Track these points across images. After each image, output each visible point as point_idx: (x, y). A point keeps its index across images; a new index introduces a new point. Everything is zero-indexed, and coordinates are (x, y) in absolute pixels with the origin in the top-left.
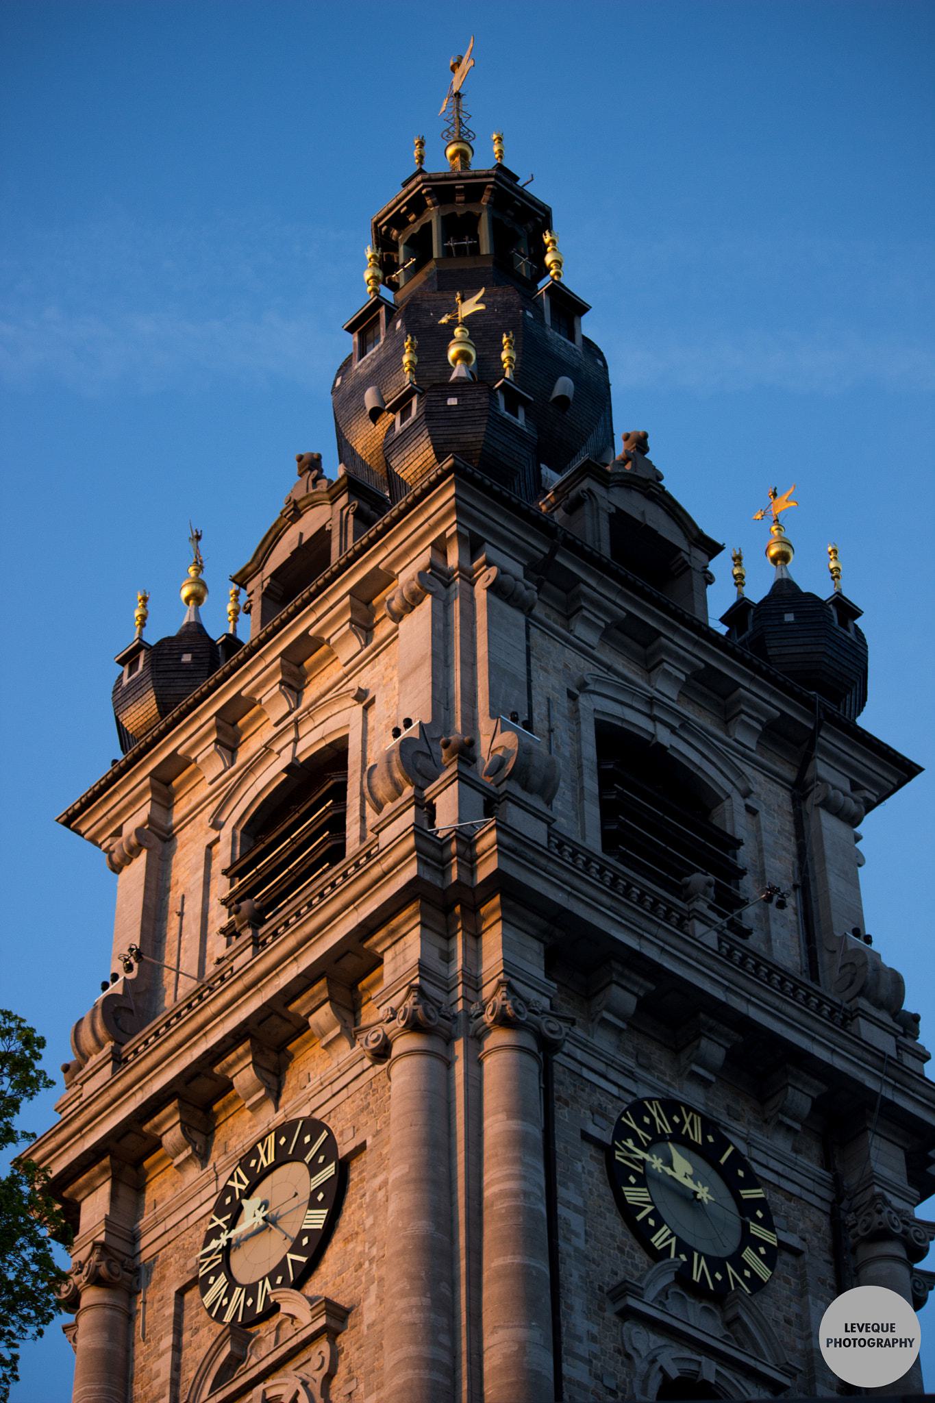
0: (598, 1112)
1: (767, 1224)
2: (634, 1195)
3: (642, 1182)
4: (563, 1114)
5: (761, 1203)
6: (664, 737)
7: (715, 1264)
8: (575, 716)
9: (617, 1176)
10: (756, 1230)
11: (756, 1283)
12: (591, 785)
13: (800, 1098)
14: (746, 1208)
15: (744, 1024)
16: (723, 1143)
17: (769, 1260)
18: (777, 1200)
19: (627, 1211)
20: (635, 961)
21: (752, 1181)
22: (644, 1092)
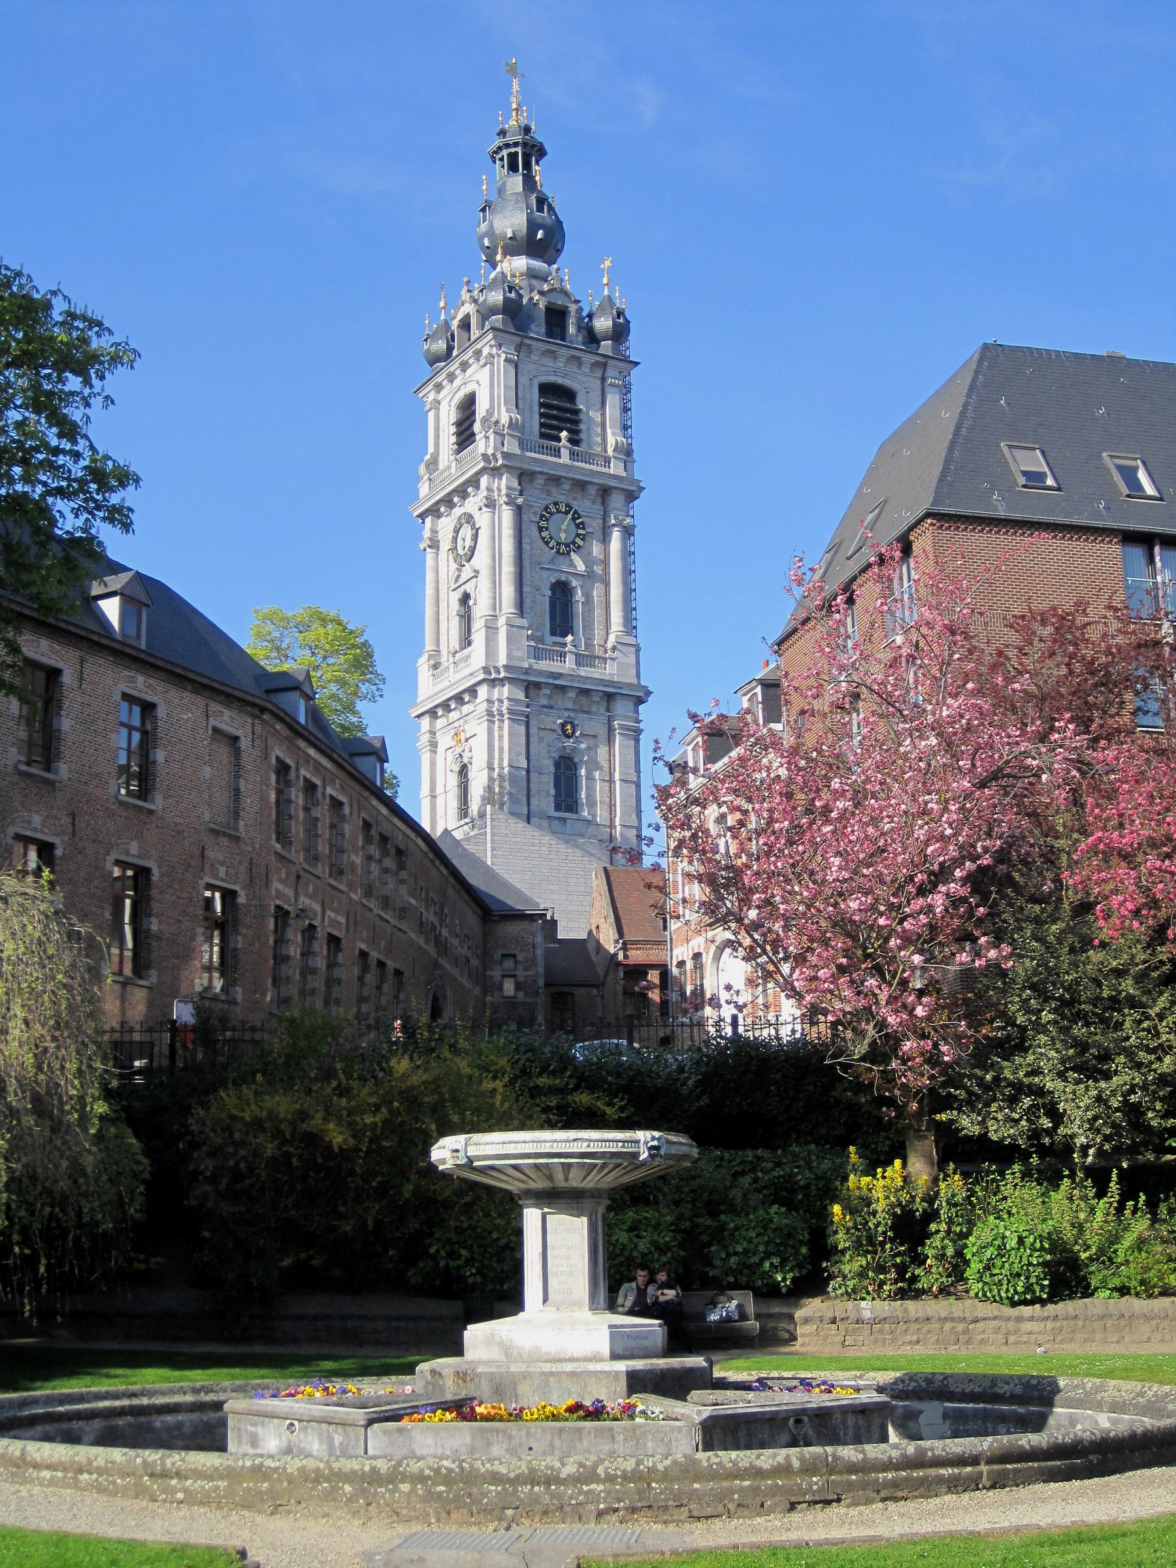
0: (535, 513)
1: (584, 529)
2: (544, 534)
3: (547, 529)
4: (525, 517)
5: (582, 523)
6: (560, 381)
7: (567, 545)
8: (531, 385)
9: (541, 529)
10: (580, 531)
11: (579, 547)
12: (536, 408)
13: (592, 490)
14: (577, 526)
15: (573, 479)
16: (571, 508)
17: (583, 539)
18: (587, 520)
19: (543, 539)
20: (541, 473)
21: (579, 517)
22: (545, 502)
